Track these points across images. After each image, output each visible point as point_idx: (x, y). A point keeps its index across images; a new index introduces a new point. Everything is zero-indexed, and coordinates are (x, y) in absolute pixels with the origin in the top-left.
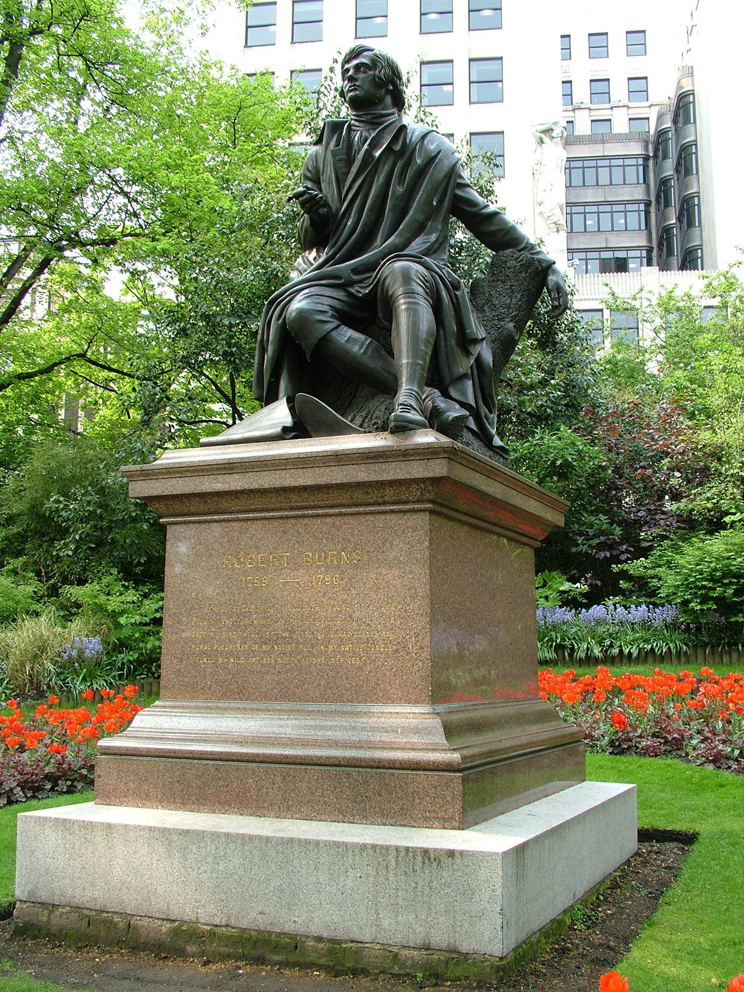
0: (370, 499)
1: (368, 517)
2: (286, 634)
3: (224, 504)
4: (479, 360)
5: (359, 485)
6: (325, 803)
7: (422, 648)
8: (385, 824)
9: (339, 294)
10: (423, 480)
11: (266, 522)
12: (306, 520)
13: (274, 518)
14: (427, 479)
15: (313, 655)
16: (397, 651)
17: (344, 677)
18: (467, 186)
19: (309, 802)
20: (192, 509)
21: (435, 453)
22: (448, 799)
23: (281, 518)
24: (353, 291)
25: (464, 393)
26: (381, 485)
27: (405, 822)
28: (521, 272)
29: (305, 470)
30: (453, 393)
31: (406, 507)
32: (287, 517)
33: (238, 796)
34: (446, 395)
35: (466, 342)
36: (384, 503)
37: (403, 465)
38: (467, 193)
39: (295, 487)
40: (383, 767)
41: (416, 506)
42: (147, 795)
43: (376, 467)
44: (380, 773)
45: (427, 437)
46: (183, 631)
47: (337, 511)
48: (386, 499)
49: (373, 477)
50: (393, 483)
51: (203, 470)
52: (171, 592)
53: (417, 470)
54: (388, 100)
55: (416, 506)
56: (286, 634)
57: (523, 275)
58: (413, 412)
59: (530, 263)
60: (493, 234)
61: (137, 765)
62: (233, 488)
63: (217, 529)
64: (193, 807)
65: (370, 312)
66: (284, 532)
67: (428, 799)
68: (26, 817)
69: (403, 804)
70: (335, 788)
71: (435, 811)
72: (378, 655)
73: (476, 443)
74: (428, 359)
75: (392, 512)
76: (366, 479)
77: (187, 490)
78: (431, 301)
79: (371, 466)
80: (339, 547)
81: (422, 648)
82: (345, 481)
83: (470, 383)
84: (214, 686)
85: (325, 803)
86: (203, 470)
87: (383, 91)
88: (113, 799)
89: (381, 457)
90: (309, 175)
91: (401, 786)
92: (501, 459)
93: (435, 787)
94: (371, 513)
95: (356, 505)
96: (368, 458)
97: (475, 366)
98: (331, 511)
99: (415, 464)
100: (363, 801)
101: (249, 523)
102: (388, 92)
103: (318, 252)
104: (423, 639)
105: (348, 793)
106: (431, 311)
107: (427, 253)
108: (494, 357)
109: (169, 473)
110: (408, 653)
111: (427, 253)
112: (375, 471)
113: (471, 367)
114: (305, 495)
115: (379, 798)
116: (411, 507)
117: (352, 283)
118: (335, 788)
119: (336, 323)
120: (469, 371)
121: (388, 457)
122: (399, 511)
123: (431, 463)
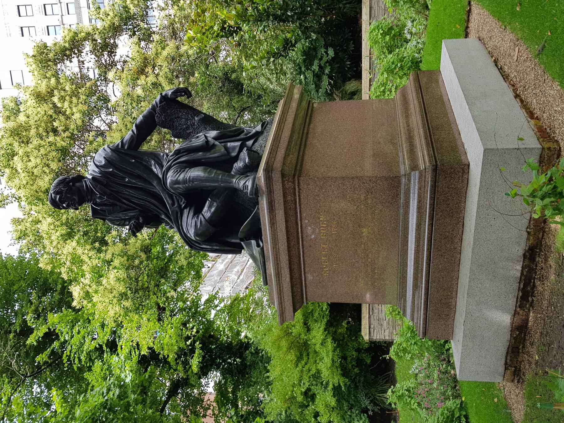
1: (302, 207)
3: (296, 275)
4: (215, 138)
6: (453, 231)
8: (465, 202)
9: (186, 212)
10: (283, 182)
11: (305, 255)
12: (304, 236)
13: (303, 252)
14: (282, 180)
16: (372, 193)
18: (122, 142)
20: (299, 290)
22: (452, 170)
23: (303, 248)
25: (234, 148)
26: (285, 202)
30: (234, 154)
31: (297, 189)
32: (303, 245)
34: (236, 159)
35: (207, 147)
36: (295, 200)
38: (126, 141)
39: (288, 243)
40: (434, 202)
42: (448, 315)
43: (277, 205)
44: (437, 204)
49: (282, 207)
50: (285, 197)
51: (280, 287)
53: (278, 187)
54: (78, 184)
56: (363, 246)
58: (247, 183)
59: (162, 108)
62: (289, 272)
63: (310, 277)
65: (194, 197)
66: (310, 246)
68: (459, 376)
71: (459, 178)
73: (260, 141)
74: (219, 172)
75: (299, 196)
76: (283, 210)
78: (187, 169)
80: (318, 221)
82: (284, 220)
83: (229, 144)
85: (453, 231)
86: (280, 287)
87: (73, 188)
89: (271, 203)
92: (268, 126)
94: (300, 206)
95: (296, 212)
96: (272, 210)
97: (220, 141)
99: (275, 187)
100: (452, 213)
101: (306, 263)
102: (73, 185)
106: (192, 169)
107: (161, 166)
108: (214, 130)
111: (161, 166)
113: (220, 143)
114: (291, 238)
115: (451, 205)
116: (297, 187)
117: (180, 206)
119: (201, 216)
120: (223, 144)
121: (272, 200)
122: (299, 192)
123: (274, 179)
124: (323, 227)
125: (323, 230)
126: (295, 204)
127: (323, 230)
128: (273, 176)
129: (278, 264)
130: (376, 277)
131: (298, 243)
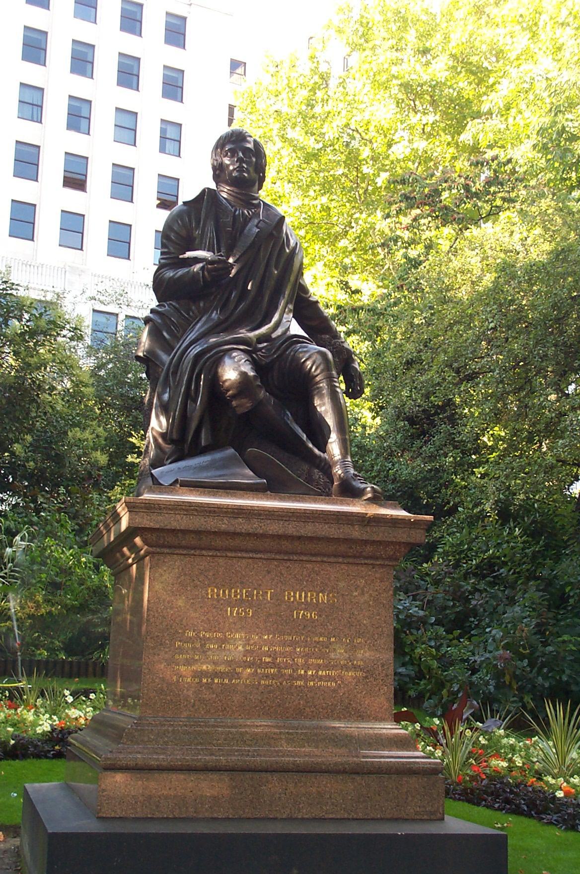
1: (343, 566)
3: (218, 542)
5: (346, 541)
12: (288, 564)
15: (294, 679)
16: (366, 677)
26: (366, 542)
33: (252, 802)
48: (364, 554)
66: (269, 572)
71: (424, 807)
84: (197, 703)
86: (210, 512)
98: (314, 559)
110: (375, 679)
114: (296, 543)
124: (306, 597)
125: (300, 596)
126: (355, 557)
127: (300, 596)
130: (205, 681)
131: (279, 552)
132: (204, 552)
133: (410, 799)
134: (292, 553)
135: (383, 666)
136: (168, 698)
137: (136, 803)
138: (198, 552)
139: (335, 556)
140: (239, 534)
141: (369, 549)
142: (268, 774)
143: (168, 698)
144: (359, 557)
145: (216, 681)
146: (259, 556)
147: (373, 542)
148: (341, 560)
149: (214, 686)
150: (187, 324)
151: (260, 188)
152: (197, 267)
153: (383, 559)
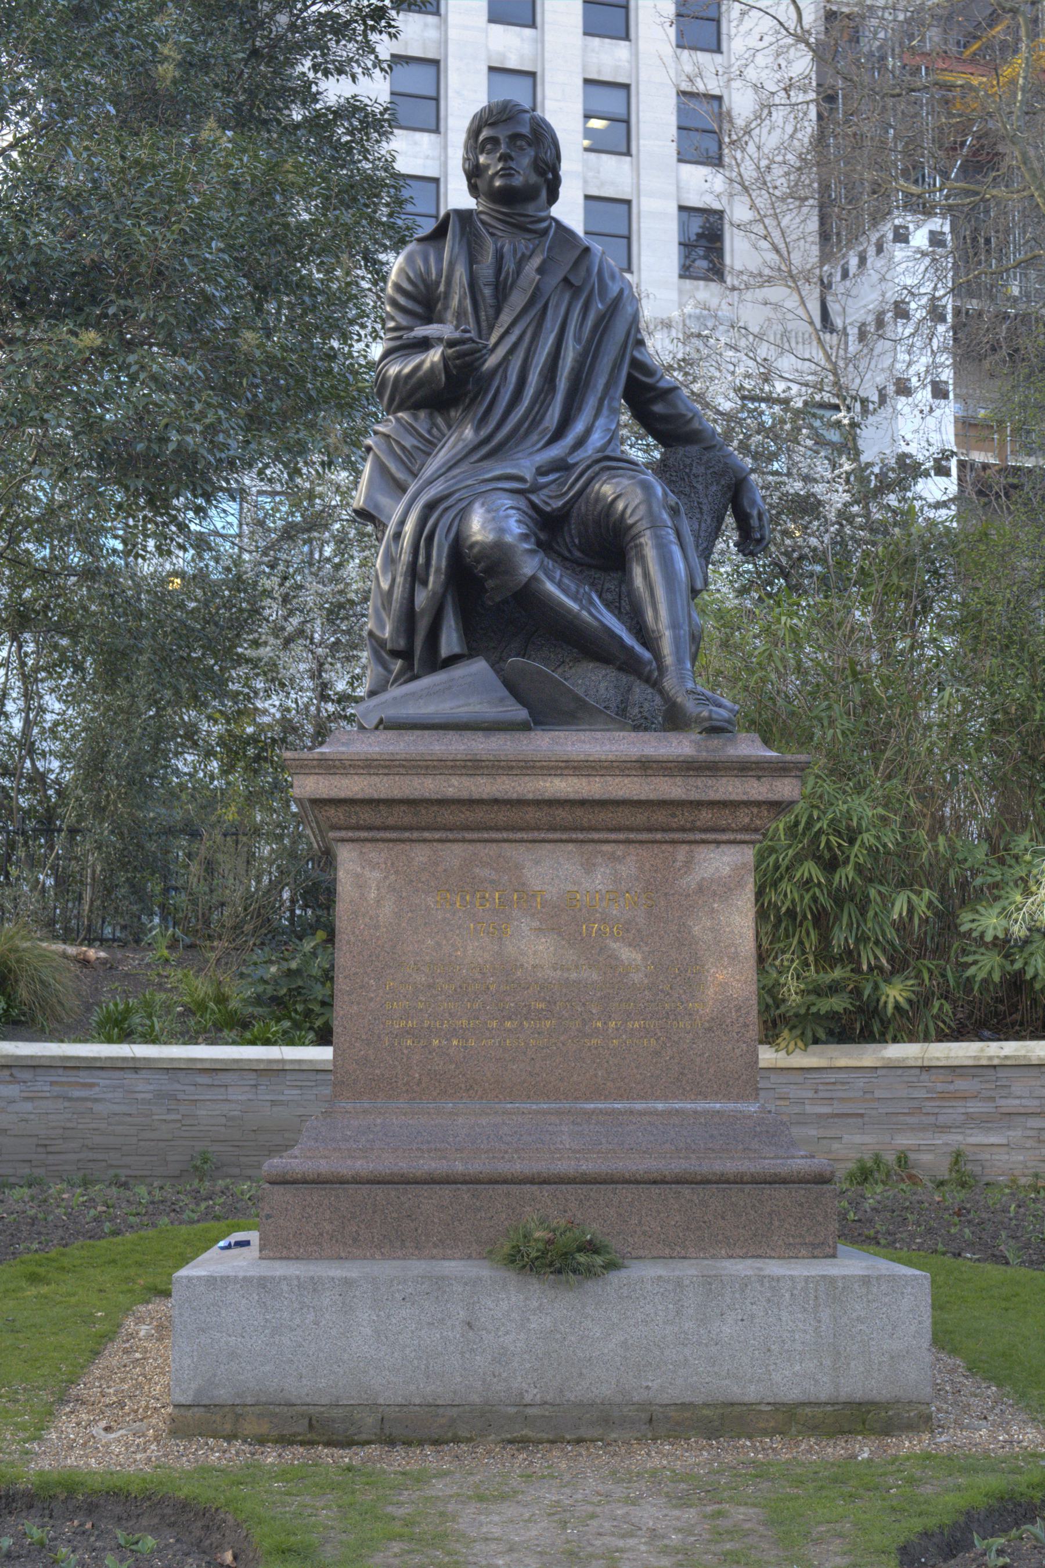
0: (674, 822)
1: (664, 847)
2: (542, 1006)
3: (447, 816)
6: (644, 1233)
7: (746, 1025)
8: (731, 1257)
10: (758, 804)
13: (522, 841)
17: (633, 1065)
19: (619, 1234)
20: (391, 821)
21: (784, 769)
22: (820, 1219)
24: (534, 498)
26: (698, 804)
27: (759, 1252)
28: (711, 484)
29: (591, 779)
37: (737, 782)
41: (740, 837)
42: (355, 1240)
43: (699, 782)
44: (724, 1190)
45: (749, 747)
46: (371, 1000)
47: (621, 836)
48: (698, 823)
52: (348, 942)
55: (740, 837)
57: (714, 488)
60: (665, 418)
61: (337, 1197)
64: (435, 1251)
67: (791, 1220)
69: (757, 1229)
70: (659, 1212)
71: (801, 1236)
72: (682, 1035)
76: (684, 797)
77: (397, 794)
79: (691, 781)
81: (746, 1025)
86: (427, 767)
88: (294, 1248)
89: (709, 769)
90: (406, 285)
91: (754, 1206)
93: (801, 1205)
96: (688, 769)
98: (613, 836)
103: (431, 416)
104: (748, 1013)
105: (677, 1218)
109: (369, 767)
110: (726, 1033)
112: (697, 787)
114: (579, 812)
117: (536, 489)
118: (659, 1212)
121: (717, 769)
126: (683, 829)
128: (787, 781)
129: (511, 768)
130: (436, 1042)
131: (553, 829)
132: (427, 835)
133: (777, 1223)
134: (575, 829)
135: (738, 1010)
136: (377, 1071)
137: (321, 1234)
138: (415, 835)
139: (649, 830)
140: (480, 802)
141: (705, 816)
142: (535, 1187)
143: (377, 1071)
144: (691, 830)
145: (455, 1043)
146: (519, 835)
147: (712, 804)
148: (659, 836)
149: (451, 1051)
150: (429, 446)
151: (553, 196)
152: (434, 356)
153: (733, 831)
